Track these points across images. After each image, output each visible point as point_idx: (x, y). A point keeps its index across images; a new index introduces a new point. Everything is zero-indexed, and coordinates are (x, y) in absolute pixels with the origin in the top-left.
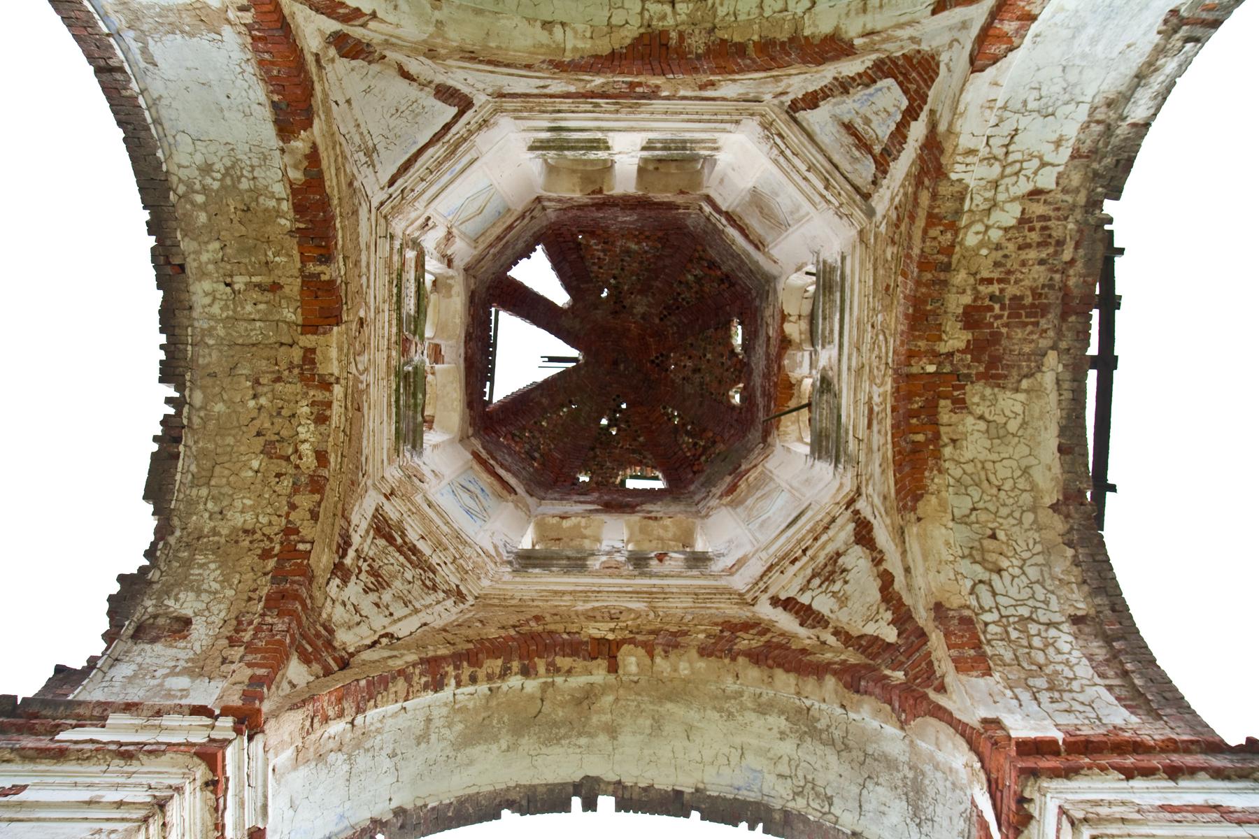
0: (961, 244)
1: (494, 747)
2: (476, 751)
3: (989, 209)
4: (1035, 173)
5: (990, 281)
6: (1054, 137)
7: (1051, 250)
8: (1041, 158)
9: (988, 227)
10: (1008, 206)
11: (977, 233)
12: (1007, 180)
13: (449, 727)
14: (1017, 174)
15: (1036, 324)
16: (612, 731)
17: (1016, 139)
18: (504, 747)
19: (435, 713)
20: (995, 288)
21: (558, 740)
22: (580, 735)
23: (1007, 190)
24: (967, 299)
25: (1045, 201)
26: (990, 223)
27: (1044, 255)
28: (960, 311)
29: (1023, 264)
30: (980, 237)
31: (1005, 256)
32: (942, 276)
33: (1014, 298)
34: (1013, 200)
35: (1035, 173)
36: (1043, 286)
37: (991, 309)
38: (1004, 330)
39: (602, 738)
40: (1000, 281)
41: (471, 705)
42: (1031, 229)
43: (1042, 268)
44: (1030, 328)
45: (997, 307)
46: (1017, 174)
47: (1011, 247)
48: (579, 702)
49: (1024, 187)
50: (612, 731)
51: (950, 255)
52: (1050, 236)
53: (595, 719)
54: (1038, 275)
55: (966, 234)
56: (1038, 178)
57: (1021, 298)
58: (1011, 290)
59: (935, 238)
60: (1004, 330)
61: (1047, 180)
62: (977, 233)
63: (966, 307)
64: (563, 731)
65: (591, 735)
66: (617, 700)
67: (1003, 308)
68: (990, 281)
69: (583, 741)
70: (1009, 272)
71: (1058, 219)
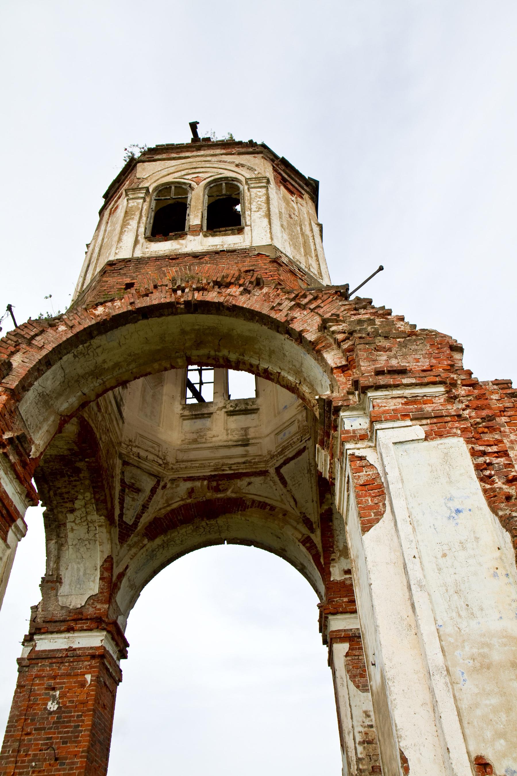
0: (91, 494)
1: (239, 332)
2: (247, 334)
3: (86, 505)
4: (75, 519)
5: (75, 481)
6: (75, 532)
7: (58, 492)
8: (75, 523)
9: (84, 499)
10: (80, 507)
11: (87, 497)
12: (84, 515)
13: (260, 349)
14: (81, 518)
15: (52, 470)
16: (183, 332)
17: (87, 530)
18: (235, 331)
19: (267, 358)
20: (72, 479)
21: (209, 328)
22: (199, 330)
23: (83, 512)
24: (81, 475)
25: (67, 508)
26: (84, 501)
27: (59, 490)
28: (82, 472)
29: (65, 487)
30: (85, 496)
31: (73, 489)
32: (94, 485)
33: (64, 477)
34: (79, 509)
35: (75, 519)
36: (55, 481)
37: (70, 473)
38: (63, 467)
39: (188, 329)
40: (72, 481)
41: (252, 353)
42: (68, 498)
43: (58, 486)
44: (54, 469)
45: (69, 474)
46: (81, 518)
47: (73, 492)
48: (201, 342)
49: (77, 513)
50: (183, 332)
51: (94, 491)
52: (60, 496)
53: (193, 336)
54: (59, 484)
55: (91, 496)
56: (74, 517)
57: (61, 477)
58: (66, 478)
59: (102, 496)
60: (63, 467)
61: (71, 517)
62: (87, 497)
63: (81, 473)
64: (207, 331)
65: (194, 330)
66: (184, 344)
67: (67, 474)
68: (75, 481)
69: (197, 327)
70: (70, 484)
71: (60, 503)
